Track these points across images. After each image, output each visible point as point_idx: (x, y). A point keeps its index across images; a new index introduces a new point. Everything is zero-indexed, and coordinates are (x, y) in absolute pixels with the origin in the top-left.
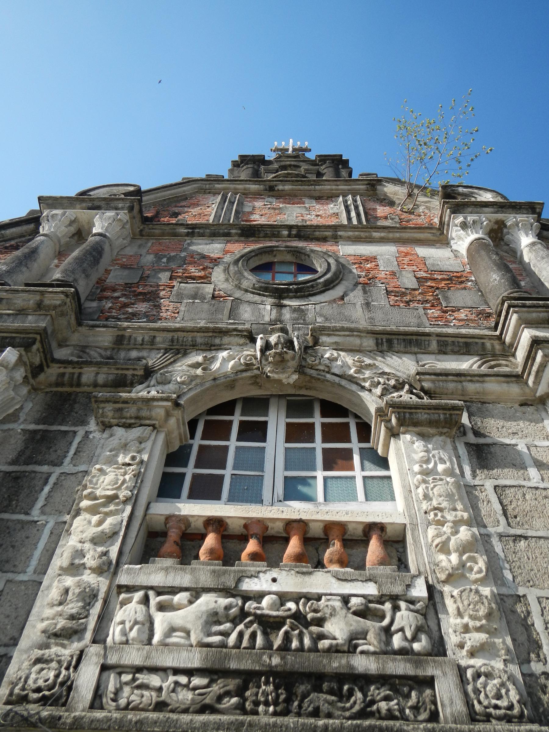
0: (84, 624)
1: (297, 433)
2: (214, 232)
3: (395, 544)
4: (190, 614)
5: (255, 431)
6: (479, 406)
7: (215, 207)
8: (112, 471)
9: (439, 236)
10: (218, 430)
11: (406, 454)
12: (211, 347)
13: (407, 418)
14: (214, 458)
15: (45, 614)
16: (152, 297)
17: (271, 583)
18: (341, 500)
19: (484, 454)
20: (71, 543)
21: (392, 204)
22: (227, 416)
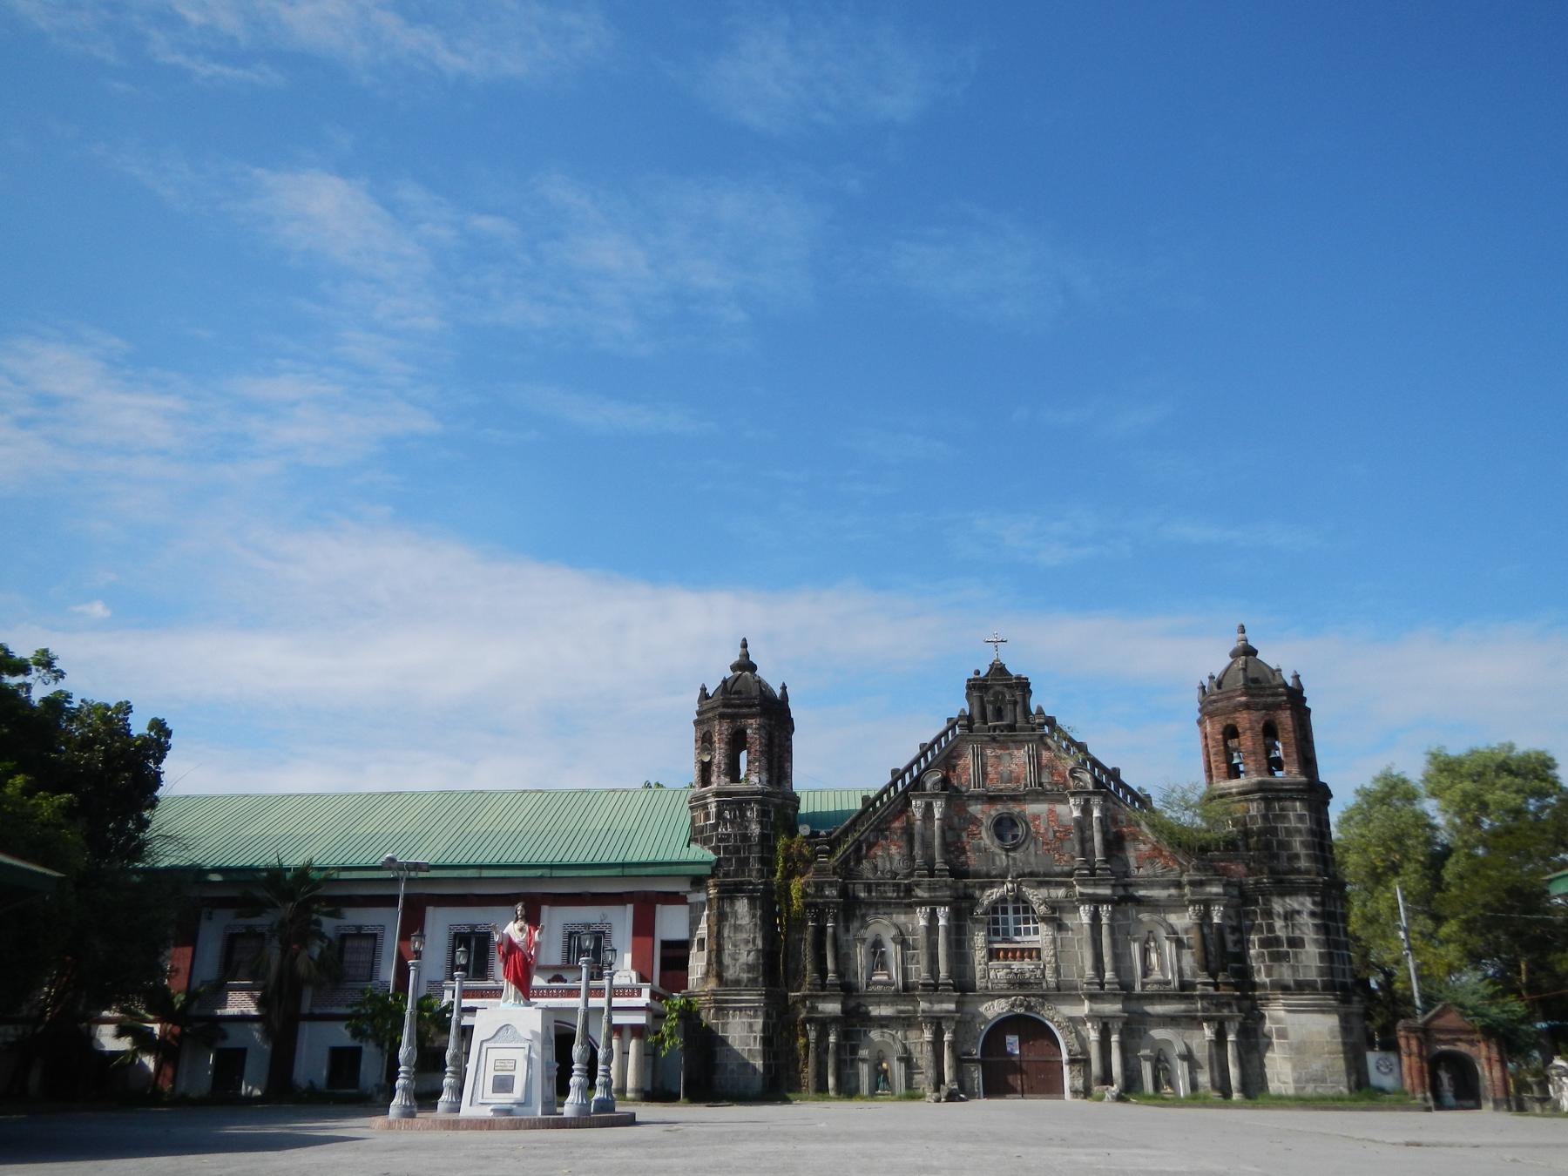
0: (986, 975)
1: (1016, 911)
2: (977, 798)
3: (1038, 950)
4: (1002, 973)
5: (1005, 911)
6: (1062, 910)
7: (970, 757)
8: (979, 939)
9: (1065, 801)
10: (995, 910)
11: (1042, 926)
12: (992, 887)
13: (1044, 919)
14: (996, 921)
15: (978, 975)
16: (964, 851)
17: (1016, 965)
18: (1026, 941)
19: (1060, 927)
20: (977, 959)
21: (1049, 749)
22: (998, 907)
